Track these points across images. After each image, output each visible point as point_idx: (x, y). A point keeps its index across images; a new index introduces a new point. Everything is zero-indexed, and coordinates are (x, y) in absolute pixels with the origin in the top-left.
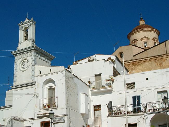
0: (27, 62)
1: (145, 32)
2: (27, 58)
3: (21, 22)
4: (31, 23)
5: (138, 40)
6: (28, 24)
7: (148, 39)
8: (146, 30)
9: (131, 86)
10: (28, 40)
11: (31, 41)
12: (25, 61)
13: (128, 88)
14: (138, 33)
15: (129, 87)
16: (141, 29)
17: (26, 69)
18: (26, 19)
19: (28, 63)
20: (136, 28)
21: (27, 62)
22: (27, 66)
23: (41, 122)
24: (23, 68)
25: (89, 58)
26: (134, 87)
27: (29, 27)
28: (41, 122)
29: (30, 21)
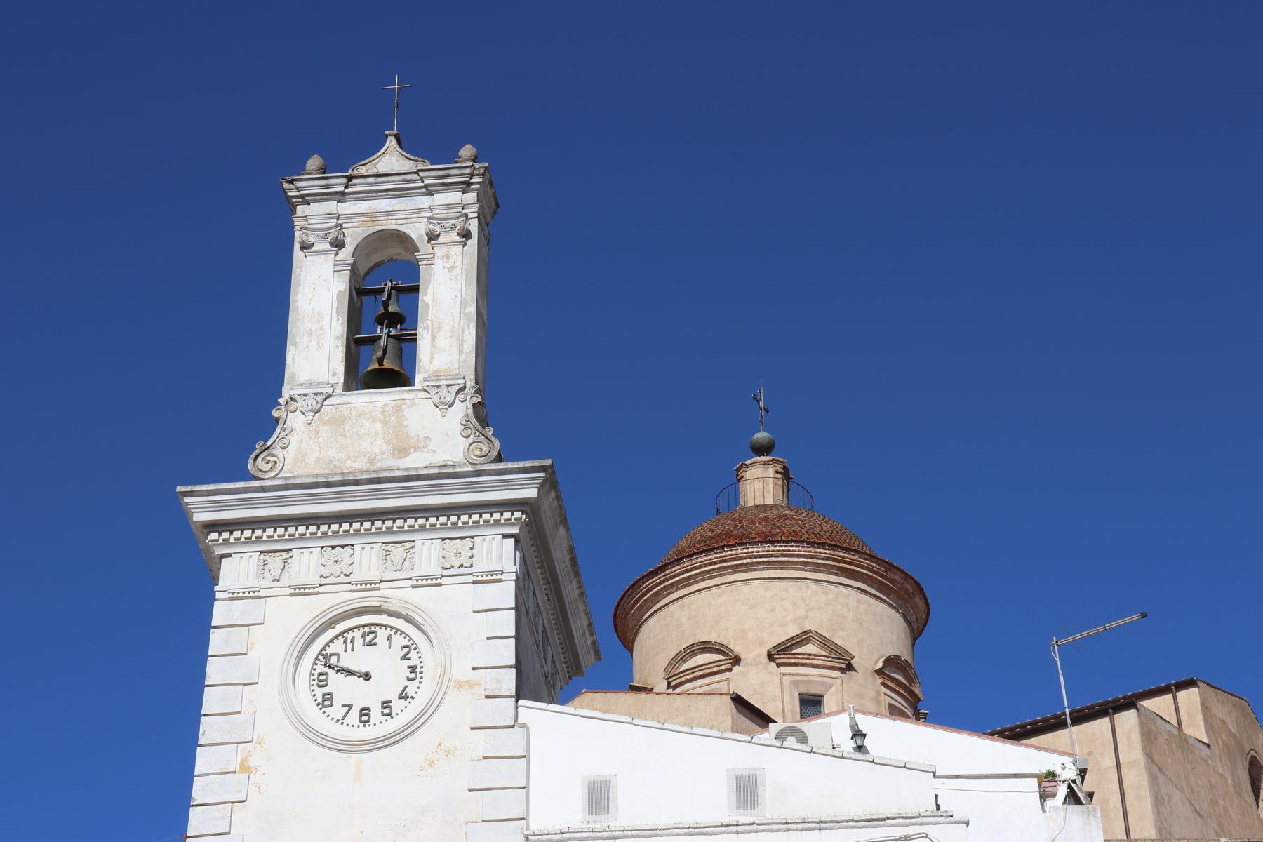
0: (398, 641)
1: (814, 587)
2: (398, 596)
3: (314, 162)
4: (454, 197)
5: (737, 661)
6: (424, 201)
8: (820, 568)
10: (418, 378)
11: (462, 409)
12: (371, 629)
14: (744, 589)
16: (780, 548)
17: (380, 727)
18: (391, 142)
19: (427, 657)
20: (729, 535)
22: (403, 696)
24: (337, 711)
27: (432, 237)
29: (457, 173)
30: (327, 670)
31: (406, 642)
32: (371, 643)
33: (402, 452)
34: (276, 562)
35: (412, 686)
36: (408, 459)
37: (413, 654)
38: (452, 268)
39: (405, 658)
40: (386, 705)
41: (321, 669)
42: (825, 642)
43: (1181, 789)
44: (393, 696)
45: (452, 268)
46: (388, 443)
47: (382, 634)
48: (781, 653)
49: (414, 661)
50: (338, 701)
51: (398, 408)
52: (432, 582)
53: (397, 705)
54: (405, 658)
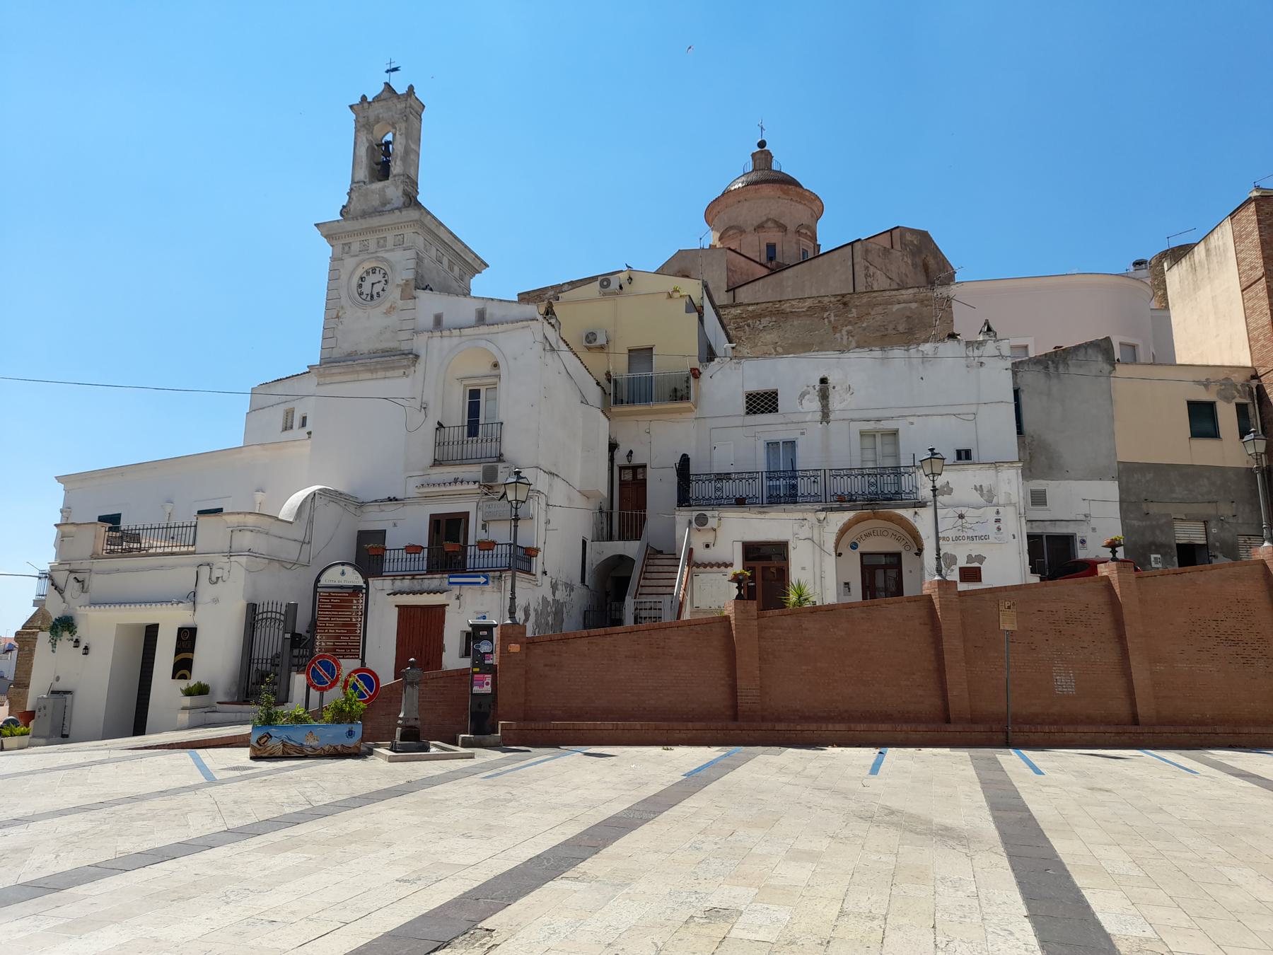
7: (783, 228)
9: (763, 402)
13: (751, 410)
15: (755, 407)
21: (385, 274)
22: (383, 290)
23: (431, 515)
24: (364, 296)
25: (605, 283)
26: (774, 408)
28: (431, 515)
30: (362, 283)
31: (384, 272)
32: (375, 273)
33: (384, 204)
36: (386, 207)
37: (386, 276)
39: (384, 277)
40: (378, 293)
41: (360, 282)
42: (776, 222)
43: (881, 270)
44: (380, 290)
46: (380, 202)
47: (378, 269)
48: (760, 227)
49: (386, 278)
52: (392, 250)
54: (384, 277)
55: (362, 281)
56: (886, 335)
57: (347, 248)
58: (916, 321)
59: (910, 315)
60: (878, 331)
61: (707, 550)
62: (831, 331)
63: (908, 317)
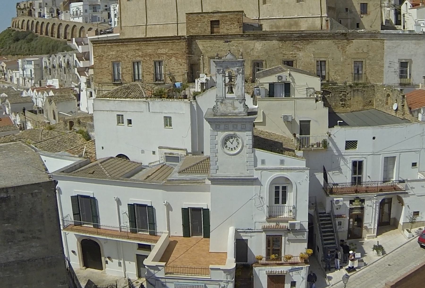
22: (237, 147)
34: (218, 127)
35: (238, 145)
38: (240, 77)
40: (235, 148)
41: (225, 142)
45: (240, 77)
47: (233, 137)
50: (228, 147)
51: (233, 102)
53: (236, 148)
54: (237, 141)
55: (226, 141)
56: (358, 53)
57: (218, 127)
58: (370, 48)
59: (368, 45)
60: (355, 50)
61: (337, 210)
62: (337, 48)
63: (368, 46)
